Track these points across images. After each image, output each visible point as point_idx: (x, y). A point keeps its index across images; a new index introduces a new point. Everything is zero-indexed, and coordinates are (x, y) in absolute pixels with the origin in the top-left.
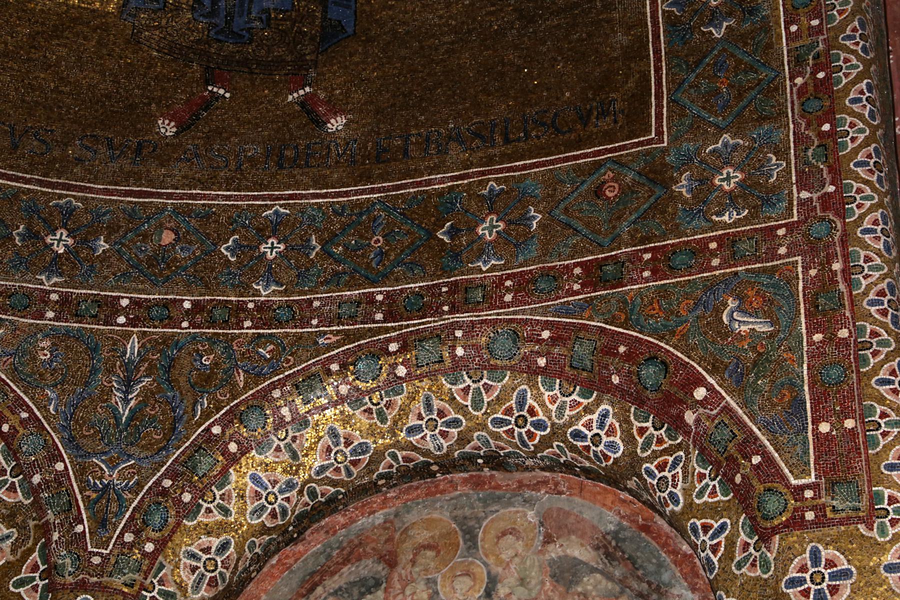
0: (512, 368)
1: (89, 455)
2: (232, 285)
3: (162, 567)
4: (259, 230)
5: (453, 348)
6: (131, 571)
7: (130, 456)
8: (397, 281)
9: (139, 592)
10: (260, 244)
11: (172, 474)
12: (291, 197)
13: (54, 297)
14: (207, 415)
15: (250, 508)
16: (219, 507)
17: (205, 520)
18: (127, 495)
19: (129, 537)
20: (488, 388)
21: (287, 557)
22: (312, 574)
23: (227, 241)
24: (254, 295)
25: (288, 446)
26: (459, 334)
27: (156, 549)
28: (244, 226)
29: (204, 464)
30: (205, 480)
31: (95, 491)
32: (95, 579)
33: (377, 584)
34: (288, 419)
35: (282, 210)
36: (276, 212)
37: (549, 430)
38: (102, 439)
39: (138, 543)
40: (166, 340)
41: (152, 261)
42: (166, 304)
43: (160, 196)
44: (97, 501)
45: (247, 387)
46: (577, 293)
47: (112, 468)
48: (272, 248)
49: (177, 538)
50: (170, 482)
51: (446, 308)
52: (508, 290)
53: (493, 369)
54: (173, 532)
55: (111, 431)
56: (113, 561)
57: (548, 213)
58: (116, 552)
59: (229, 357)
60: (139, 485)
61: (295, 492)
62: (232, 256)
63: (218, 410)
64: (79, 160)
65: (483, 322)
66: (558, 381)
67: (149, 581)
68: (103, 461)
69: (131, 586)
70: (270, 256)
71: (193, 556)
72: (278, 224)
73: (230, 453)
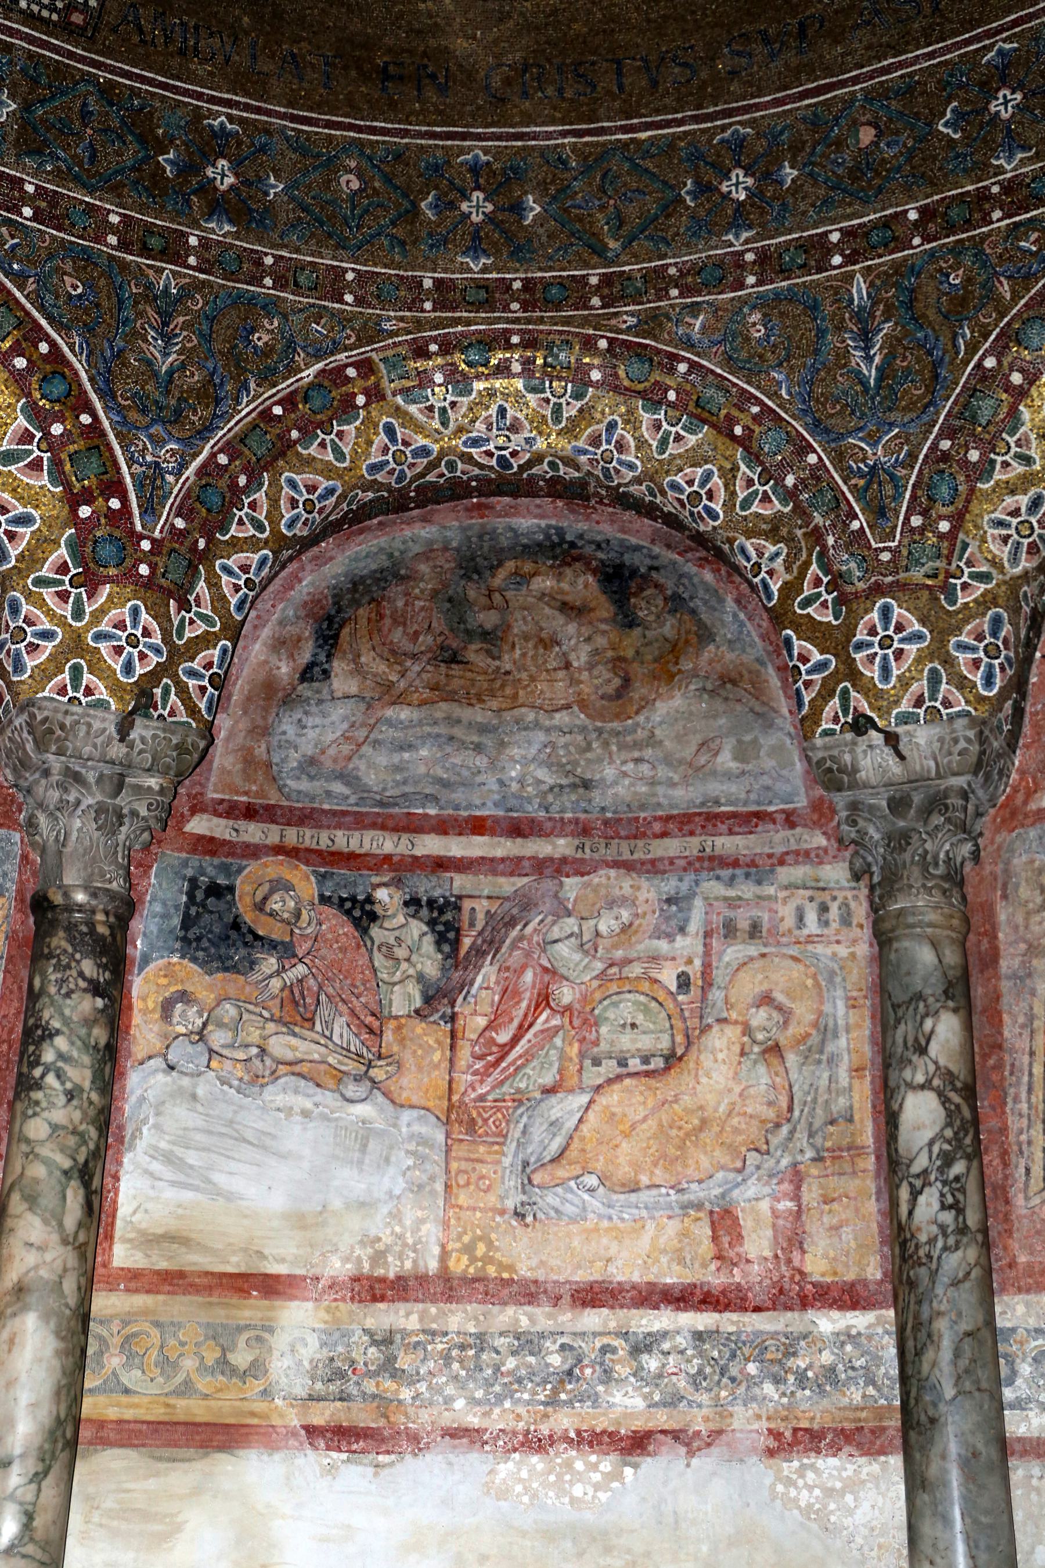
1: (841, 436)
2: (965, 170)
3: (965, 546)
4: (982, 84)
6: (930, 559)
7: (891, 425)
9: (946, 582)
10: (988, 103)
11: (949, 432)
12: (1015, 23)
13: (750, 257)
14: (972, 348)
16: (1018, 456)
17: (1004, 477)
18: (901, 472)
19: (916, 521)
23: (944, 114)
24: (996, 175)
27: (953, 527)
28: (961, 86)
29: (985, 408)
30: (991, 428)
31: (862, 477)
32: (890, 579)
35: (1007, 46)
36: (1001, 52)
38: (853, 412)
39: (929, 525)
40: (897, 267)
41: (855, 173)
42: (886, 223)
43: (843, 84)
44: (867, 488)
45: (1016, 297)
47: (874, 444)
48: (1006, 103)
49: (974, 506)
50: (949, 443)
54: (968, 501)
55: (861, 400)
56: (905, 552)
58: (906, 541)
59: (984, 266)
60: (912, 456)
62: (955, 132)
63: (986, 337)
64: (733, 73)
67: (954, 565)
68: (861, 439)
69: (935, 576)
70: (1005, 115)
71: (1001, 524)
72: (1006, 67)
73: (1015, 387)
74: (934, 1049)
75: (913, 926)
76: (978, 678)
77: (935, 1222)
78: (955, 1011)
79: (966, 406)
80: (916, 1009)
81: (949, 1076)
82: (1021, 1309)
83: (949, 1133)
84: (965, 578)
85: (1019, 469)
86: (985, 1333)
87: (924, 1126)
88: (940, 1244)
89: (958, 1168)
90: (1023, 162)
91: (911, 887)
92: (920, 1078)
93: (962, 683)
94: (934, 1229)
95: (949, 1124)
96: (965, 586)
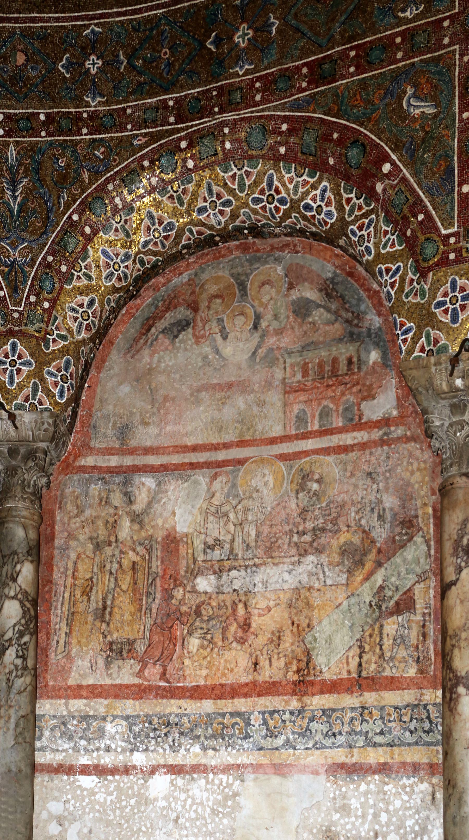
0: (263, 157)
2: (70, 98)
3: (56, 319)
4: (83, 48)
5: (223, 142)
6: (38, 322)
7: (24, 240)
8: (182, 88)
9: (45, 336)
10: (85, 61)
11: (52, 252)
12: (102, 16)
14: (68, 206)
15: (104, 275)
16: (85, 274)
17: (78, 284)
18: (27, 269)
20: (248, 174)
21: (131, 308)
22: (148, 319)
23: (61, 60)
24: (86, 106)
25: (122, 227)
26: (226, 130)
27: (50, 306)
28: (72, 45)
29: (71, 243)
30: (73, 255)
31: (7, 266)
32: (17, 328)
33: (188, 324)
34: (120, 206)
35: (97, 29)
36: (93, 31)
37: (289, 204)
38: (4, 227)
39: (39, 303)
40: (33, 146)
44: (9, 273)
46: (304, 90)
47: (14, 249)
48: (94, 64)
49: (62, 297)
50: (52, 258)
51: (216, 109)
52: (258, 90)
53: (251, 158)
54: (59, 293)
55: (9, 221)
56: (26, 315)
57: (283, 19)
58: (27, 309)
59: (76, 159)
61: (130, 262)
62: (67, 73)
63: (75, 201)
65: (242, 119)
66: (293, 165)
67: (49, 328)
68: (7, 244)
69: (40, 332)
70: (93, 72)
71: (74, 310)
72: (96, 41)
73: (87, 235)
74: (20, 579)
75: (15, 517)
76: (56, 392)
77: (13, 663)
78: (32, 562)
79: (62, 239)
80: (13, 559)
81: (26, 594)
82: (48, 706)
83: (23, 621)
84: (54, 336)
85: (85, 282)
86: (31, 717)
87: (12, 617)
88: (14, 674)
89: (26, 638)
90: (100, 103)
91: (16, 496)
92: (12, 594)
93: (49, 393)
94: (12, 667)
95: (23, 617)
96: (54, 340)
